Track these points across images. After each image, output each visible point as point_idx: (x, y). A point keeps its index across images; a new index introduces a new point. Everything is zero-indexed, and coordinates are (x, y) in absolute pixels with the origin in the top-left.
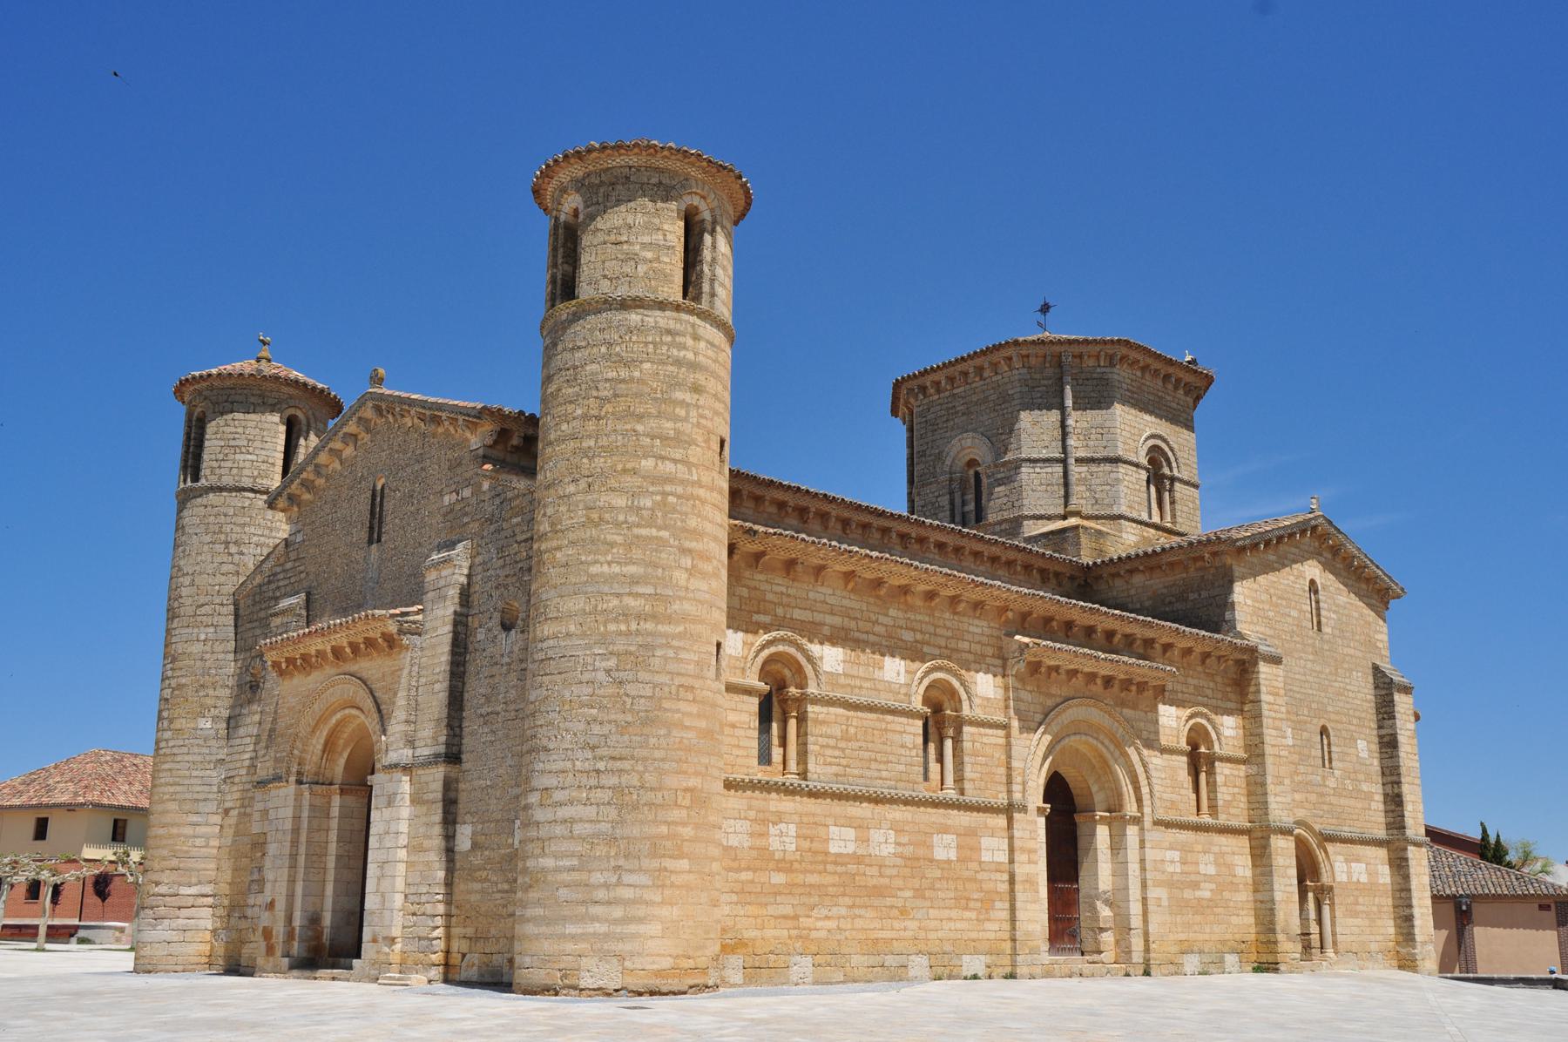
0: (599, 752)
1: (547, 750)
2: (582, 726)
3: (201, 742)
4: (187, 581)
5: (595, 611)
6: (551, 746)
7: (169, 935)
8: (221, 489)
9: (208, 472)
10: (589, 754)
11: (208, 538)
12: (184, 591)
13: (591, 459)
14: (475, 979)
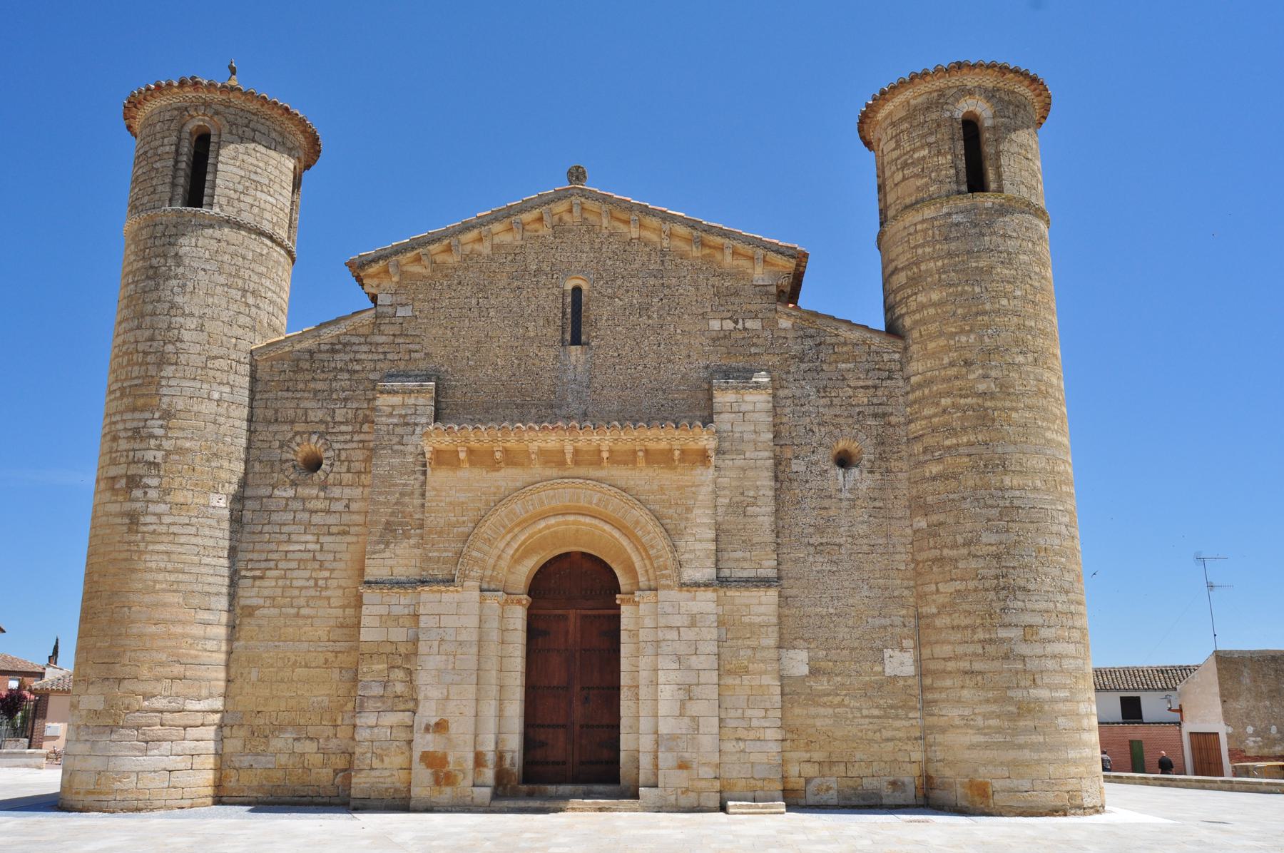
1: (1024, 589)
2: (1057, 572)
3: (214, 523)
4: (192, 323)
6: (1030, 587)
7: (172, 762)
8: (239, 226)
9: (223, 201)
11: (222, 279)
12: (186, 335)
13: (1034, 337)
14: (834, 801)
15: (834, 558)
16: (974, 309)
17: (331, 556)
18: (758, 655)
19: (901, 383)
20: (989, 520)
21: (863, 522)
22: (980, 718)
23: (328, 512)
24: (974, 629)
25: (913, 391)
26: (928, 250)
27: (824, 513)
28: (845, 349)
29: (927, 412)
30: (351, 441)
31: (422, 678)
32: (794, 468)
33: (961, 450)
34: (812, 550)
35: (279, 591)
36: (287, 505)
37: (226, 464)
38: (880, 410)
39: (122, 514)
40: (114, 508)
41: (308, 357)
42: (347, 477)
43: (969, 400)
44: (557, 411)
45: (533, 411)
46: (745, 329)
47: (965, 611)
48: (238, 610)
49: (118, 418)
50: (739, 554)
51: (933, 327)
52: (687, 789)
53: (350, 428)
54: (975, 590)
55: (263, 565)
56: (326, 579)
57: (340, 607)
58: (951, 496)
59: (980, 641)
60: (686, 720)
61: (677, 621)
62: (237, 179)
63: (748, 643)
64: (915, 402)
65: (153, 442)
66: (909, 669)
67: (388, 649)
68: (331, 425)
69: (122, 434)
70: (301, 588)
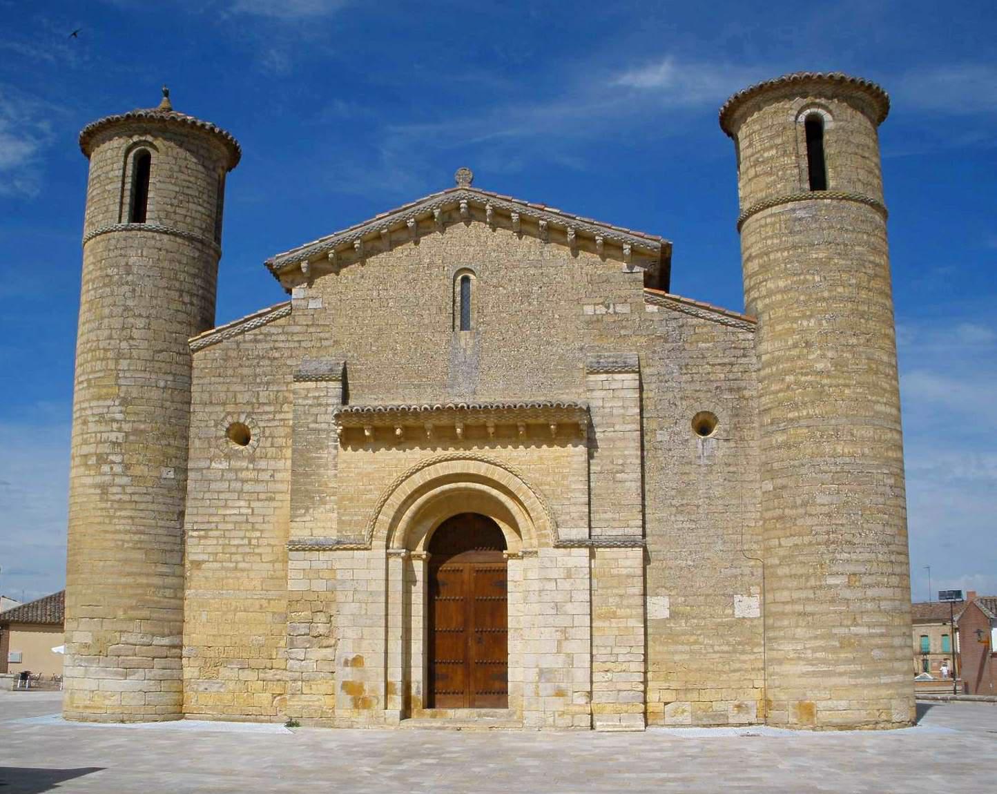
0: (892, 548)
2: (880, 527)
5: (879, 440)
10: (886, 549)
11: (164, 283)
15: (693, 517)
16: (814, 296)
17: (260, 519)
18: (625, 602)
19: (754, 360)
20: (823, 484)
21: (718, 485)
22: (809, 651)
23: (257, 481)
24: (808, 578)
25: (763, 368)
26: (776, 241)
27: (685, 478)
28: (705, 330)
29: (774, 387)
30: (273, 420)
31: (339, 621)
32: (659, 438)
33: (803, 422)
34: (674, 509)
35: (220, 549)
36: (223, 475)
37: (172, 442)
38: (734, 385)
39: (96, 486)
40: (89, 481)
41: (234, 346)
42: (271, 452)
43: (809, 378)
44: (449, 390)
45: (429, 390)
46: (615, 313)
47: (801, 563)
48: (188, 565)
49: (85, 405)
50: (609, 515)
51: (781, 312)
52: (563, 713)
53: (272, 409)
54: (810, 544)
55: (205, 526)
56: (258, 538)
57: (270, 562)
58: (792, 463)
59: (812, 588)
60: (562, 657)
61: (554, 574)
62: (173, 195)
63: (615, 591)
64: (765, 378)
65: (115, 425)
66: (756, 612)
67: (313, 597)
68: (257, 406)
69: (91, 419)
70: (238, 546)
